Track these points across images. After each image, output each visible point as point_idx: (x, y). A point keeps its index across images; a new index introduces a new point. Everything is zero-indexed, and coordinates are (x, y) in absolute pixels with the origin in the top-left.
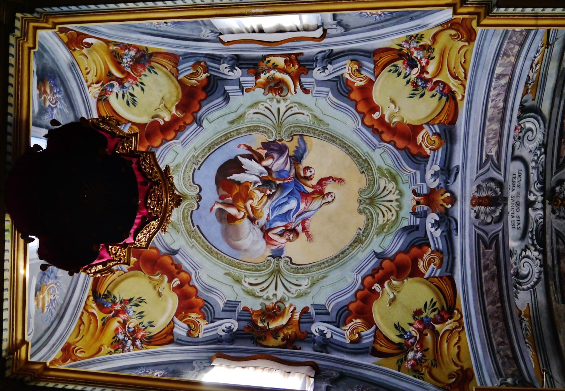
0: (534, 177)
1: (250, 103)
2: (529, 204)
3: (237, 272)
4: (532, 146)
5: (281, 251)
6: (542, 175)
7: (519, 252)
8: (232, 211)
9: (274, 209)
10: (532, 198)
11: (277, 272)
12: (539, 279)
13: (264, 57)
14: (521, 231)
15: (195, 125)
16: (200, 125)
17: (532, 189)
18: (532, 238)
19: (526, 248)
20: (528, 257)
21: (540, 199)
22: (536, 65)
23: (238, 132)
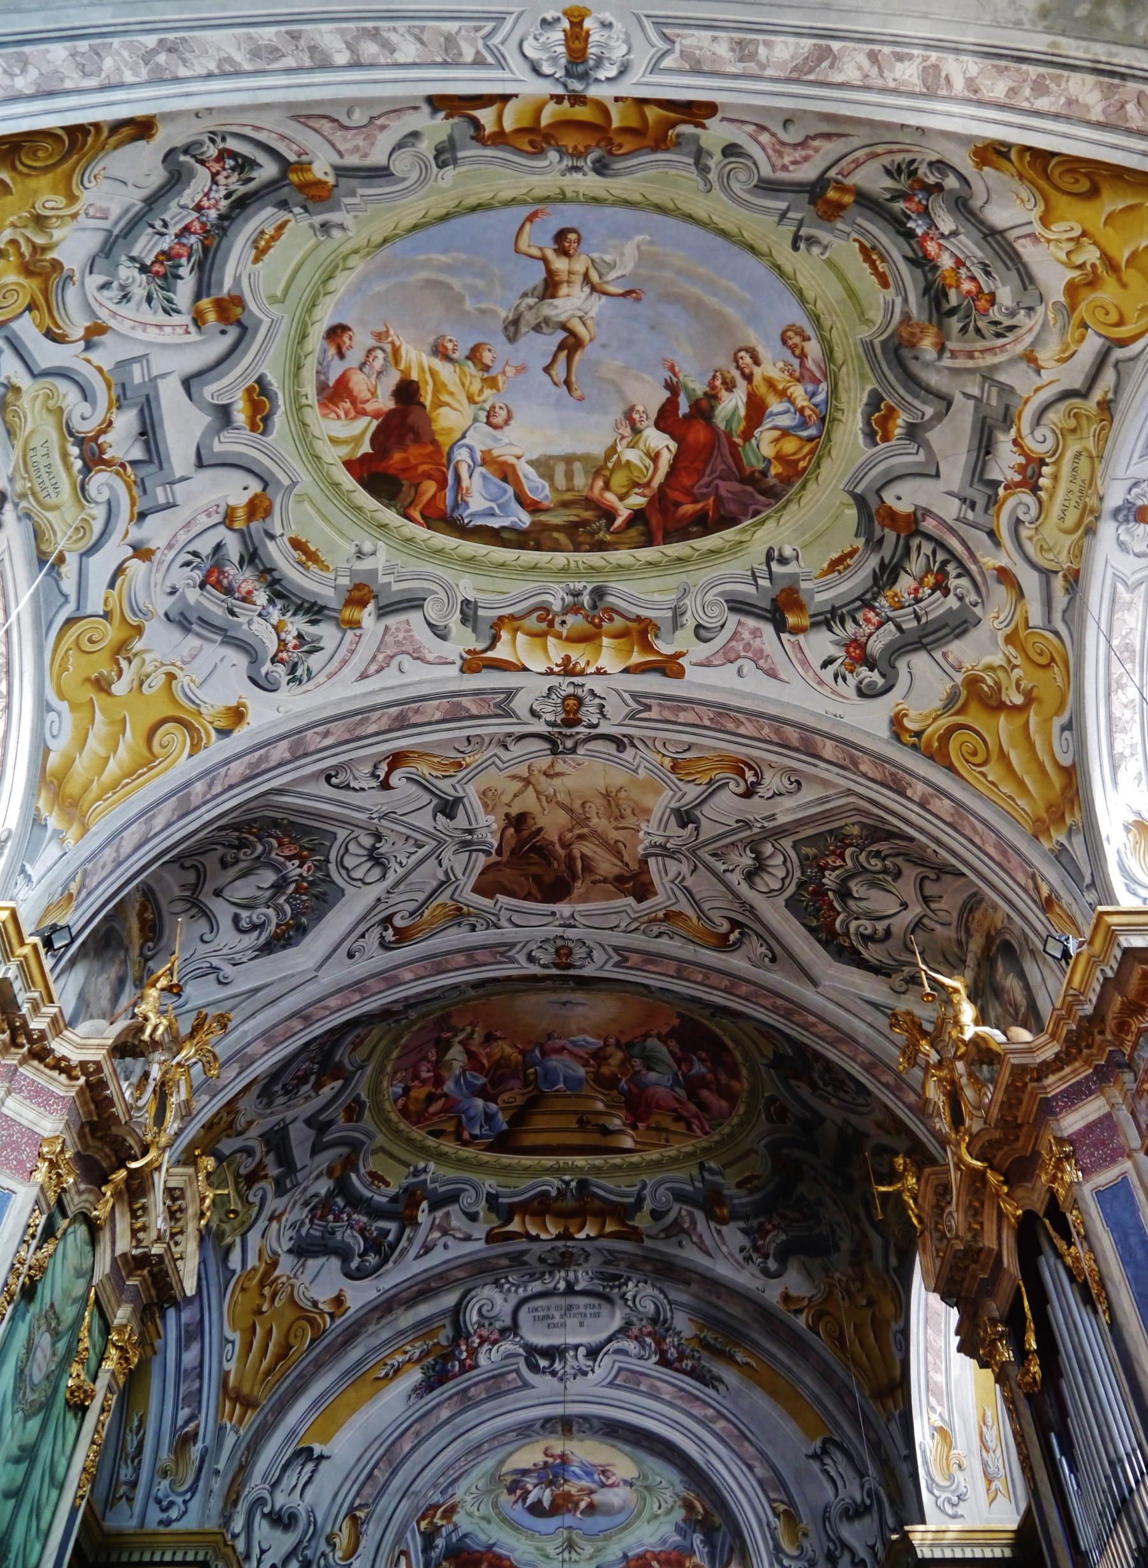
0: (536, 1287)
1: (469, 1519)
2: (570, 1290)
3: (646, 1514)
4: (498, 1298)
5: (625, 1482)
6: (533, 1277)
7: (628, 1310)
8: (583, 1505)
9: (578, 1477)
10: (562, 1286)
11: (647, 1488)
12: (661, 1291)
13: (421, 1533)
14: (603, 1303)
15: (495, 1549)
16: (494, 1545)
17: (551, 1286)
18: (612, 1288)
19: (623, 1297)
20: (634, 1297)
21: (563, 1274)
22: (406, 1352)
23: (499, 1514)
